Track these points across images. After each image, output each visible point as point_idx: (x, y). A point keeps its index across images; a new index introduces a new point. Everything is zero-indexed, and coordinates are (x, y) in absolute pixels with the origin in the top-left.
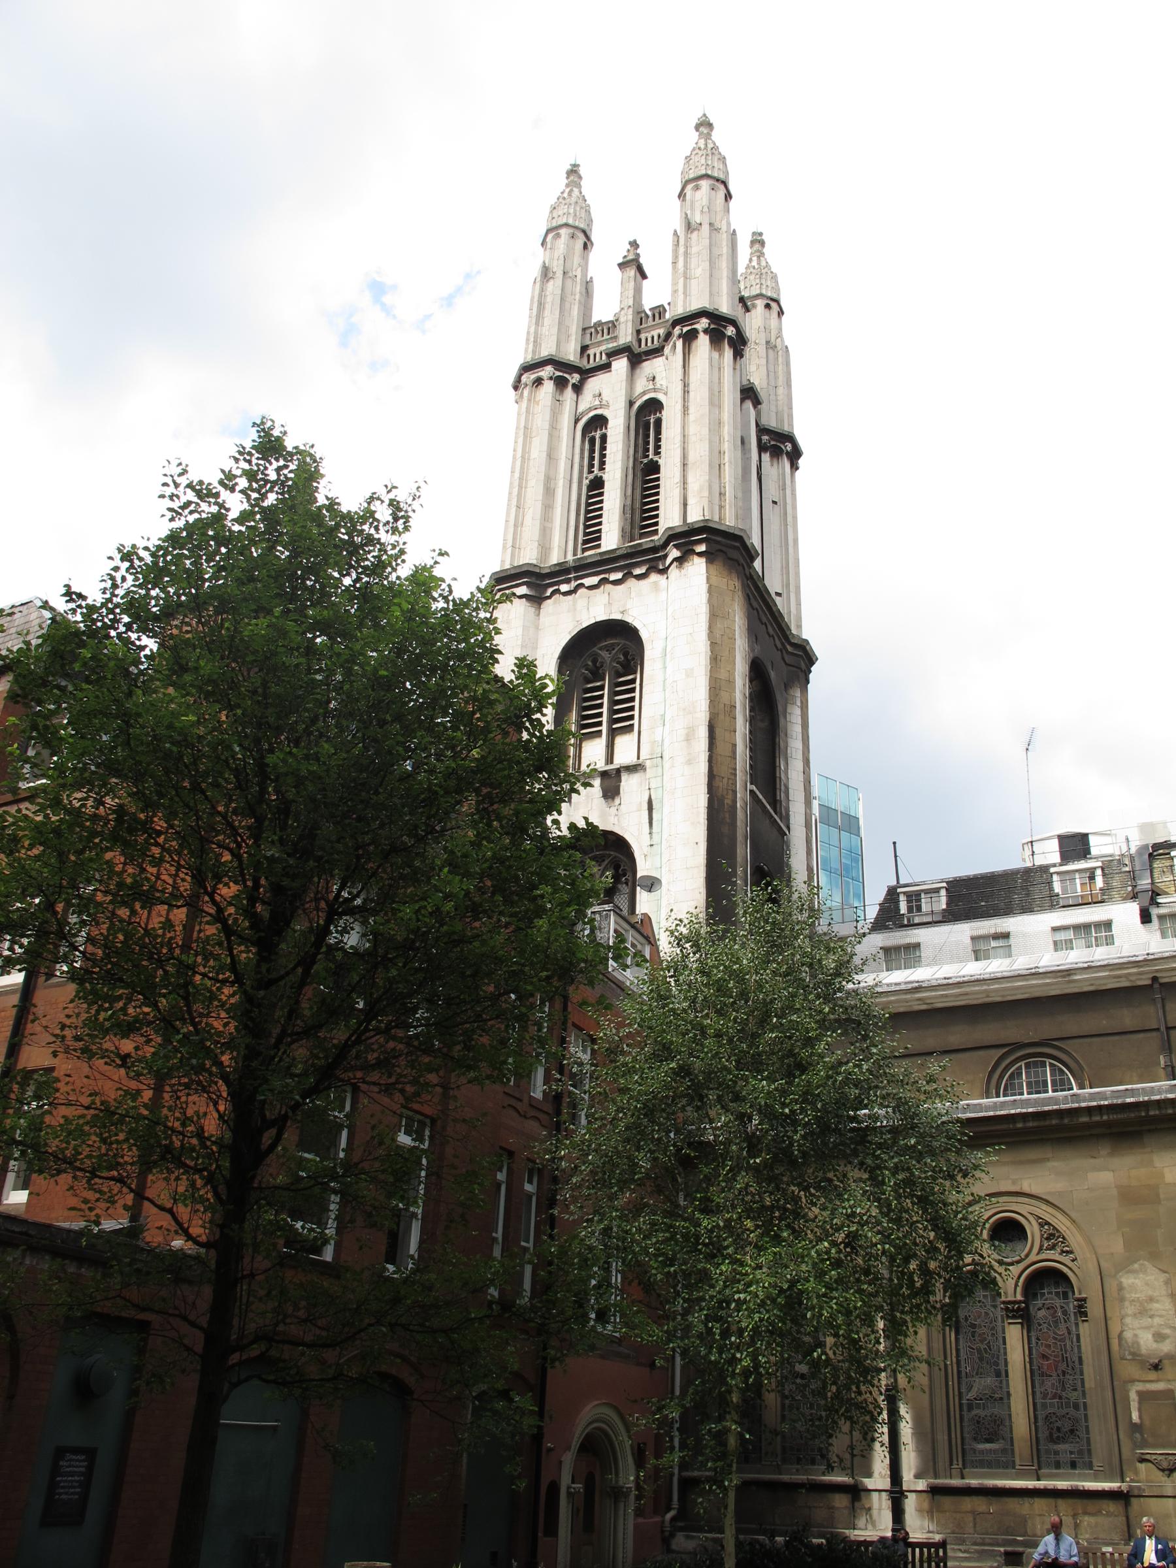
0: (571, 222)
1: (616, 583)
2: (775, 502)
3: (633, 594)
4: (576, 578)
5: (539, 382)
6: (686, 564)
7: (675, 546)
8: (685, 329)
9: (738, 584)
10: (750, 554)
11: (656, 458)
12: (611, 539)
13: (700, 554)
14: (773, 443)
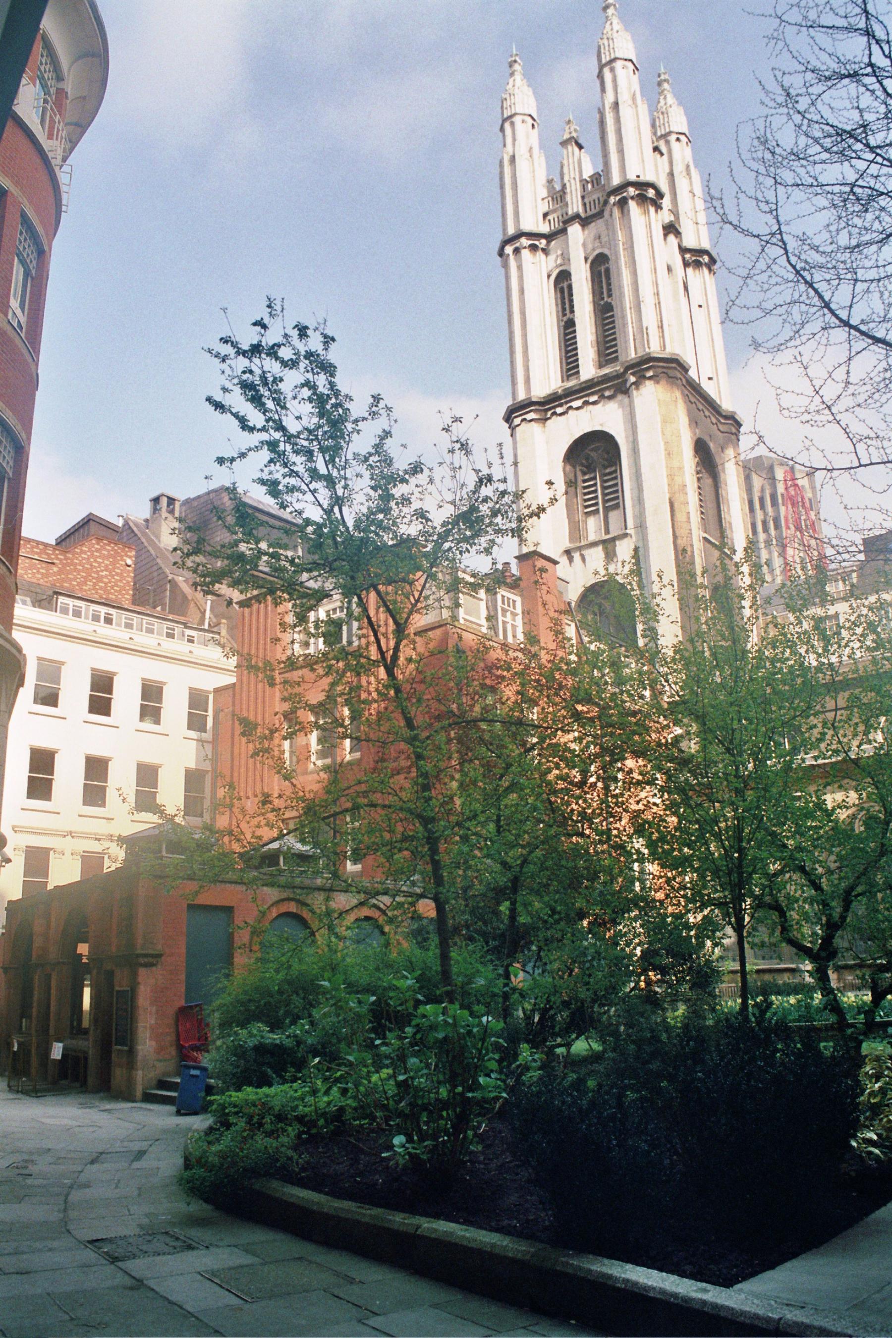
2: (700, 306)
4: (567, 403)
5: (517, 251)
7: (633, 374)
8: (618, 198)
9: (678, 394)
10: (685, 369)
12: (588, 369)
13: (650, 378)
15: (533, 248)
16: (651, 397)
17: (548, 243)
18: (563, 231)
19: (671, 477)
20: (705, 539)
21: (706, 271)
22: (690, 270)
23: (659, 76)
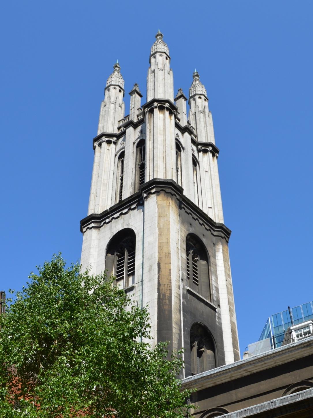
0: (113, 83)
1: (126, 213)
2: (206, 171)
3: (132, 216)
4: (112, 216)
5: (100, 145)
6: (149, 198)
7: (145, 193)
10: (180, 190)
11: (144, 162)
13: (154, 193)
14: (203, 148)
15: (109, 142)
16: (153, 202)
17: (118, 139)
18: (124, 133)
19: (161, 247)
20: (188, 291)
21: (210, 155)
22: (201, 154)
23: (194, 73)
